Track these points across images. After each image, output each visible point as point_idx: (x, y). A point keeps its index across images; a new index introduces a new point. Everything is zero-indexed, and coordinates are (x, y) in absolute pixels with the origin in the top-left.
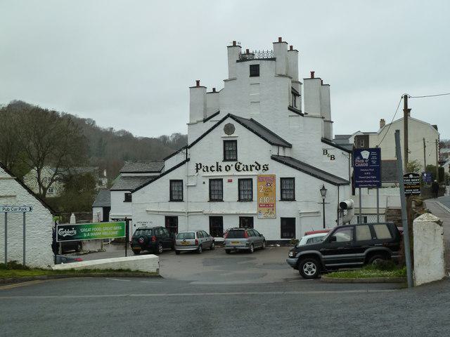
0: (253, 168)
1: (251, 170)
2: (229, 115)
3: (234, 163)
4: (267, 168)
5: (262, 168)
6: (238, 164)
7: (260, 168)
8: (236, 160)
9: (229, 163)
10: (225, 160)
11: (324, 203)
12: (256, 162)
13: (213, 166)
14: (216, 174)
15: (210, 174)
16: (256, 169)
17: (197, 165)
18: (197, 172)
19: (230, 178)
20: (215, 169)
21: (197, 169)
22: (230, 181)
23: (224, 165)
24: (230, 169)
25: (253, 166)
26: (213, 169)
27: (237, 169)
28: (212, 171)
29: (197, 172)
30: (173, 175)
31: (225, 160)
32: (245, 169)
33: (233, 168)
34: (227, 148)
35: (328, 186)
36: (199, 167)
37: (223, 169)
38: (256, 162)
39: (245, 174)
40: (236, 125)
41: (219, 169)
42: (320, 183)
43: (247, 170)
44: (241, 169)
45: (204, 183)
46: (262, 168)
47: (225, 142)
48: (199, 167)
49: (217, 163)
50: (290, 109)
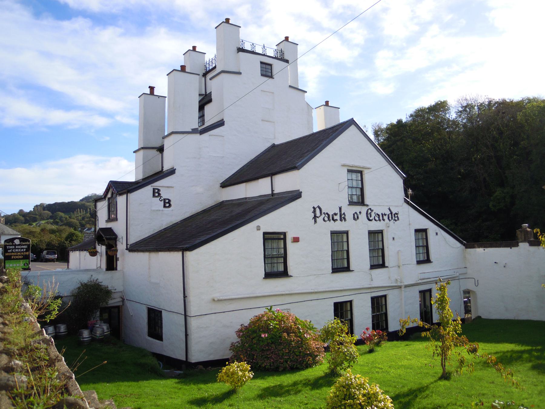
0: (386, 218)
9: (357, 209)
13: (336, 214)
14: (339, 226)
17: (314, 208)
18: (315, 222)
20: (337, 217)
23: (349, 211)
25: (385, 215)
26: (335, 217)
28: (335, 220)
29: (315, 222)
39: (375, 226)
41: (343, 218)
44: (373, 215)
49: (340, 209)
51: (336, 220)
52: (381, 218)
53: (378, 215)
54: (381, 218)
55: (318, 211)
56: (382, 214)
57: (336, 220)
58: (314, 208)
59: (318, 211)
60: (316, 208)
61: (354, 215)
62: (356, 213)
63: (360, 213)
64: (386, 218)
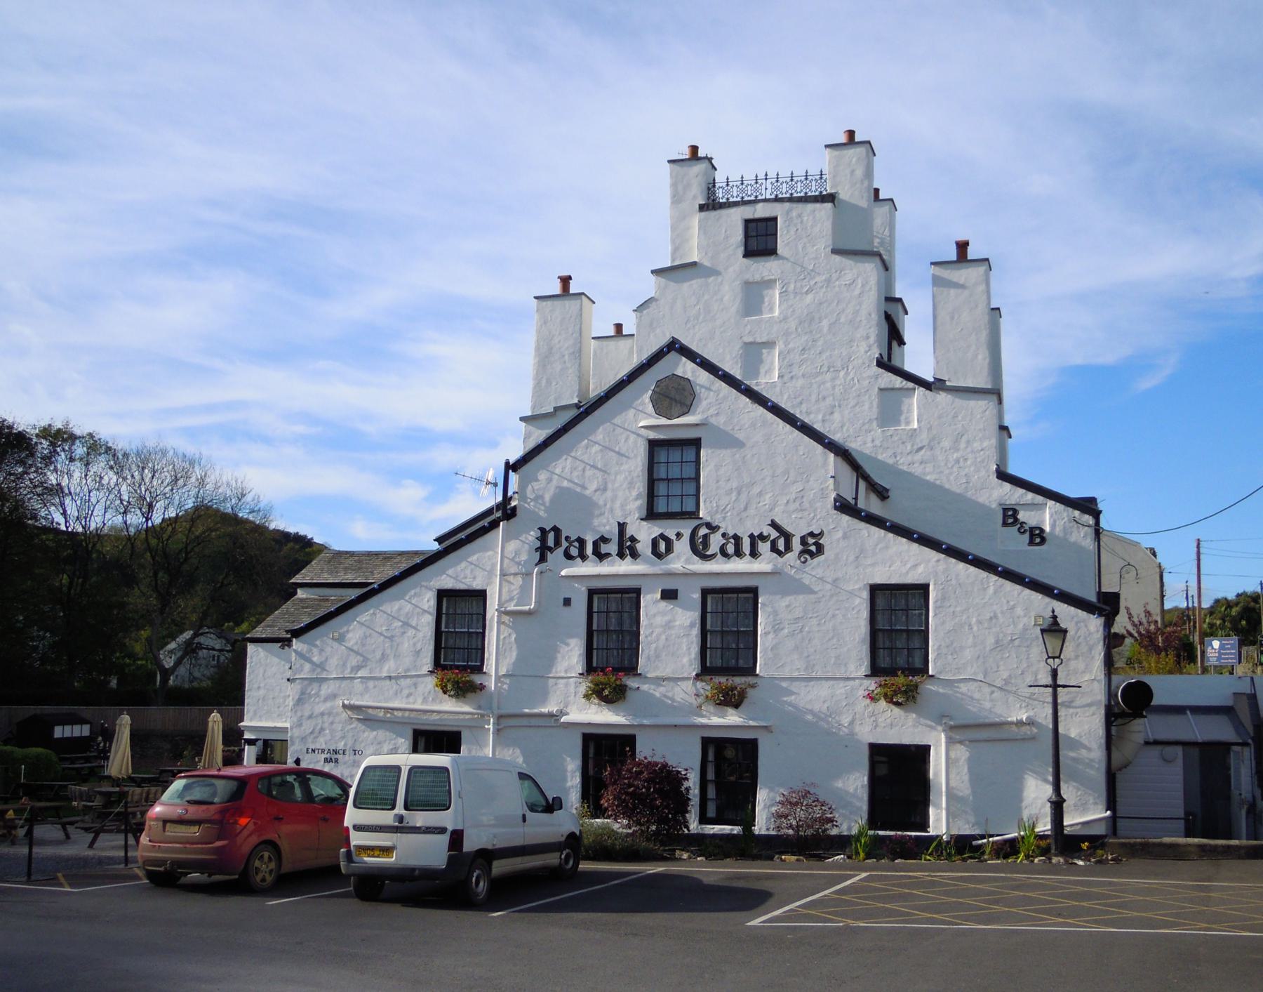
0: (764, 547)
1: (754, 554)
2: (675, 347)
3: (686, 528)
4: (820, 549)
5: (796, 545)
6: (703, 531)
7: (788, 548)
8: (694, 515)
9: (670, 529)
10: (651, 514)
11: (1055, 686)
12: (774, 525)
13: (604, 540)
15: (590, 568)
16: (774, 549)
17: (543, 530)
18: (543, 559)
19: (670, 585)
20: (612, 548)
21: (543, 551)
22: (670, 595)
23: (645, 533)
24: (669, 549)
25: (762, 537)
26: (604, 549)
27: (700, 549)
29: (543, 559)
30: (456, 574)
31: (651, 514)
32: (730, 549)
33: (682, 547)
34: (661, 472)
35: (1067, 614)
36: (551, 543)
37: (644, 547)
38: (774, 525)
40: (702, 377)
41: (628, 548)
42: (1041, 604)
43: (739, 553)
44: (716, 541)
45: (567, 602)
46: (796, 545)
47: (653, 445)
48: (551, 543)
49: (622, 527)
50: (880, 364)
51: (608, 555)
52: (746, 547)
53: (737, 539)
54: (746, 547)
55: (551, 536)
56: (751, 536)
57: (608, 555)
58: (543, 530)
59: (551, 536)
60: (550, 531)
61: (655, 543)
62: (662, 536)
63: (679, 535)
64: (764, 547)
